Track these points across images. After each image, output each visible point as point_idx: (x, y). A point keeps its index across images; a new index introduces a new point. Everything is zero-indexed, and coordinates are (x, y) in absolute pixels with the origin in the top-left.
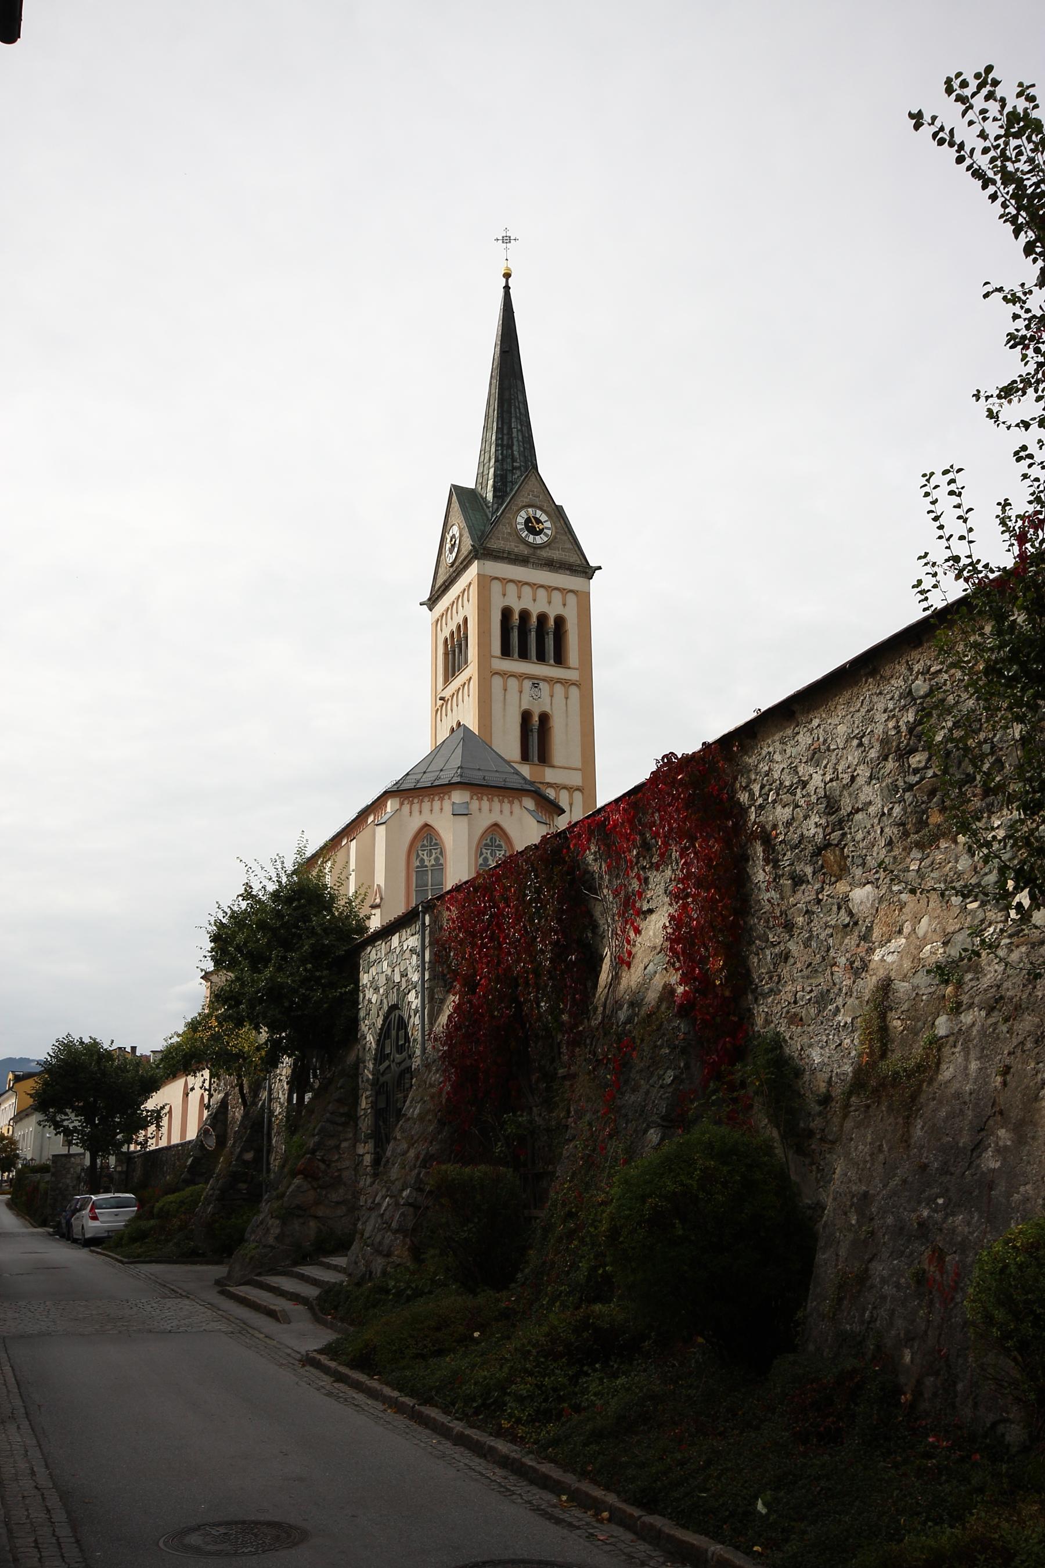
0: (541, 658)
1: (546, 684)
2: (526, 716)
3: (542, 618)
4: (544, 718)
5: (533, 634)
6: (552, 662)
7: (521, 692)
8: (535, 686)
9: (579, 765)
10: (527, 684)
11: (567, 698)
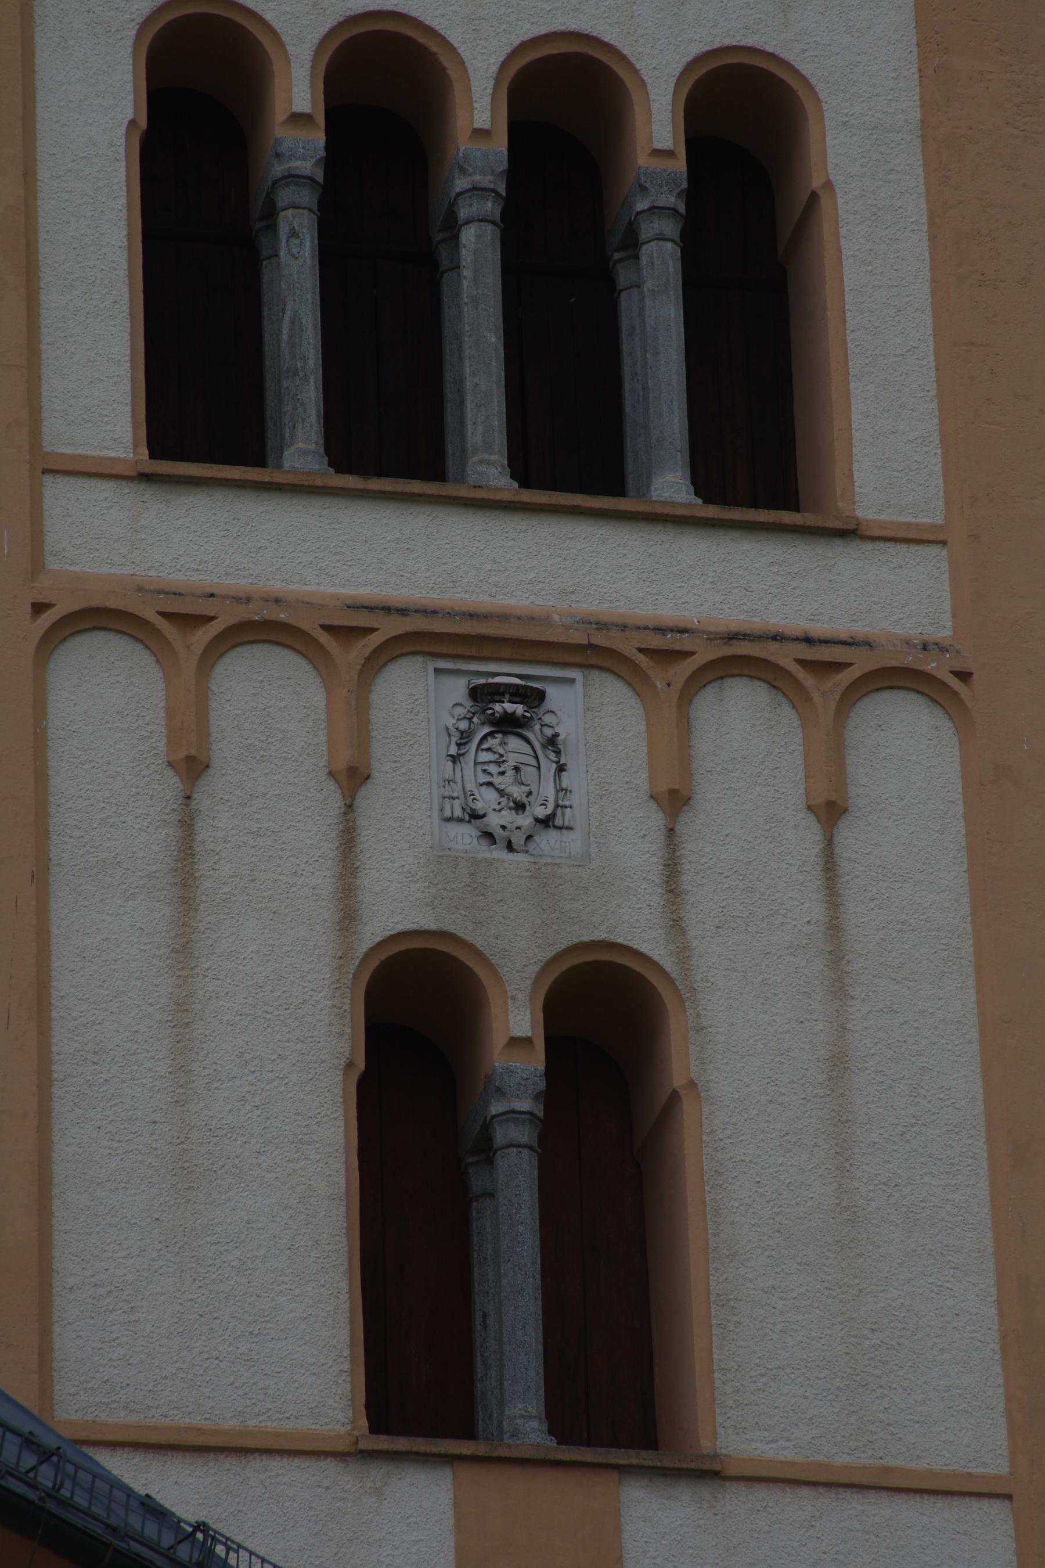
0: (570, 456)
1: (612, 694)
2: (412, 1018)
3: (566, 97)
4: (610, 1024)
5: (476, 257)
6: (672, 485)
7: (353, 778)
8: (506, 712)
9: (973, 1436)
10: (420, 703)
11: (830, 812)
